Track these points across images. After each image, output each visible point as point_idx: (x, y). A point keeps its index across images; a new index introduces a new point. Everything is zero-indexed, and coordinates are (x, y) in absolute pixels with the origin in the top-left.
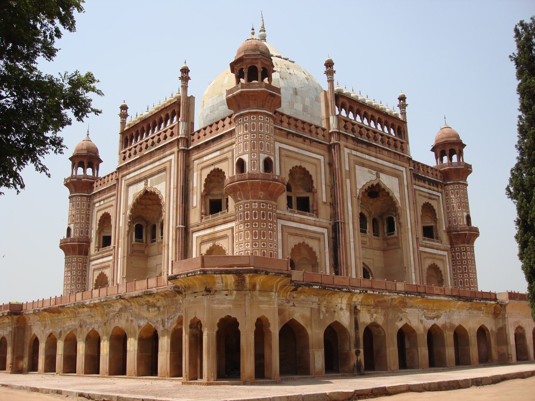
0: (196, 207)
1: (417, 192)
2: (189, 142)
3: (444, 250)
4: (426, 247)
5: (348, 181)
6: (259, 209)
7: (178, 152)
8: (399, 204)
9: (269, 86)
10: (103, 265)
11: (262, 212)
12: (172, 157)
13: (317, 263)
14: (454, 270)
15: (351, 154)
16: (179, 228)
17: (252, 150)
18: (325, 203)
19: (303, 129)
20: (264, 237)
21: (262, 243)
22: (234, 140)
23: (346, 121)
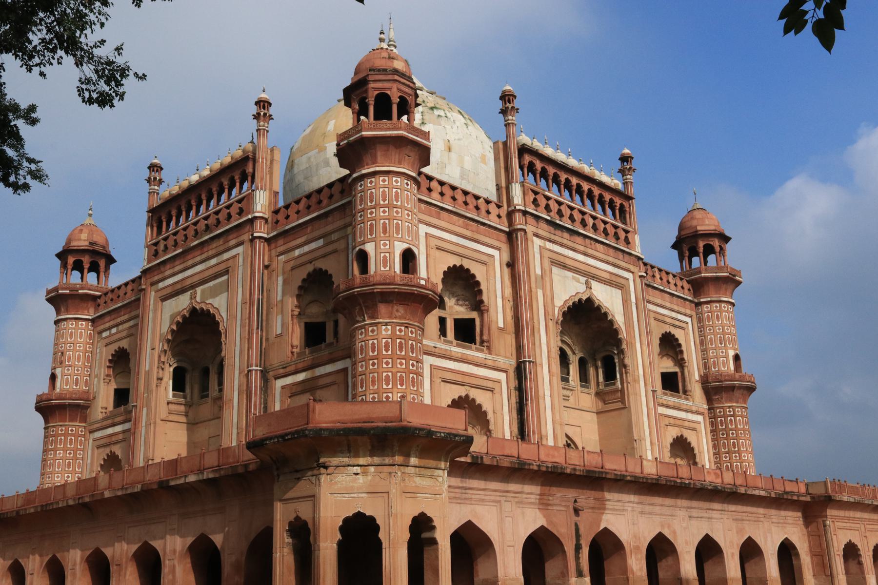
0: (281, 335)
1: (652, 315)
3: (697, 413)
4: (668, 407)
5: (540, 293)
6: (393, 337)
8: (623, 335)
9: (411, 128)
10: (114, 439)
11: (398, 341)
12: (240, 249)
14: (715, 447)
17: (382, 235)
18: (501, 330)
19: (466, 203)
20: (402, 385)
22: (348, 220)
23: (536, 193)
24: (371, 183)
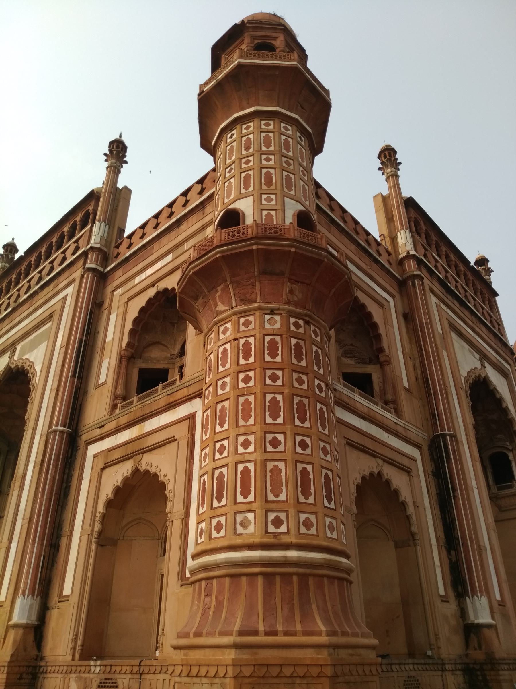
0: (104, 384)
2: (110, 260)
5: (445, 354)
11: (294, 341)
12: (70, 290)
13: (413, 535)
15: (440, 306)
16: (55, 432)
17: (264, 187)
20: (303, 421)
21: (298, 439)
23: (426, 250)
24: (247, 128)
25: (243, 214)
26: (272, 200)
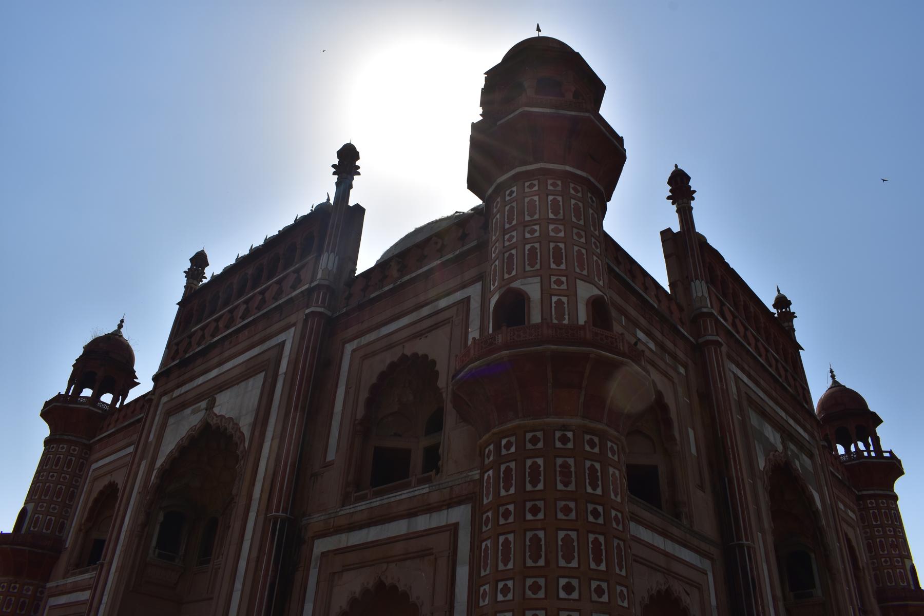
7: (306, 321)
16: (276, 519)
25: (529, 298)
26: (563, 283)
